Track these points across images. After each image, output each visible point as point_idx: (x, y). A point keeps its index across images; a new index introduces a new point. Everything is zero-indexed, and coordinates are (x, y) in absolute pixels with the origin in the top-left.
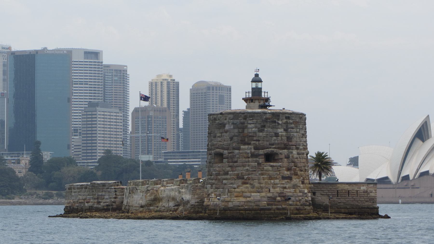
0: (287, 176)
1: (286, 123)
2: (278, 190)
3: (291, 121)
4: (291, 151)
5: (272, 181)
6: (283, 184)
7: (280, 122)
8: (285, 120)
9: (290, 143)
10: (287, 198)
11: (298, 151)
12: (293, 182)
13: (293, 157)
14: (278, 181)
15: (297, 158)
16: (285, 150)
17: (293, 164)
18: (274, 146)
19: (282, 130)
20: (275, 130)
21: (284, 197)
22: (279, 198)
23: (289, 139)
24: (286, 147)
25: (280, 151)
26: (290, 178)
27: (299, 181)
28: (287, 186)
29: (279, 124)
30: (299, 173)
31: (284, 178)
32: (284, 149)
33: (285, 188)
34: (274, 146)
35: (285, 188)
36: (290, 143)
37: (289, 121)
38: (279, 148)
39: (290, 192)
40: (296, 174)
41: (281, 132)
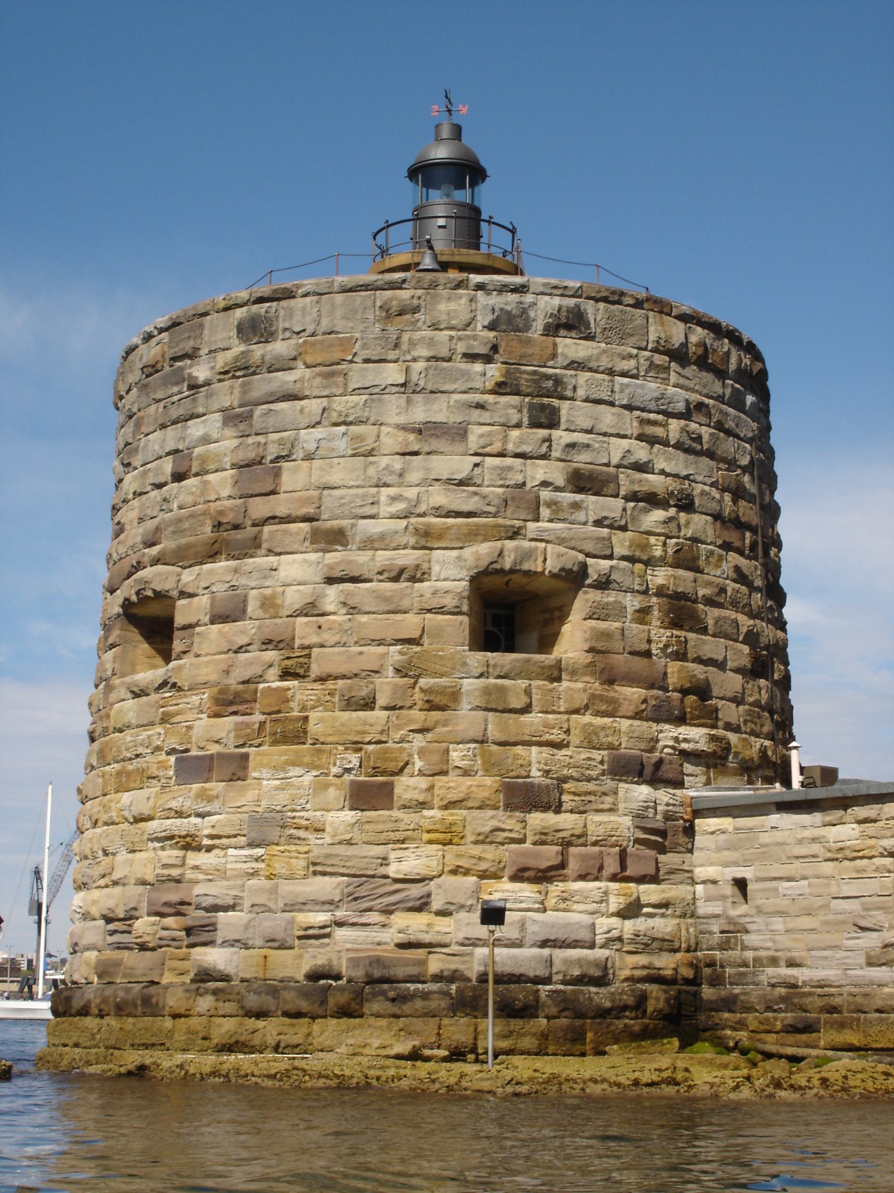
0: (214, 749)
1: (242, 369)
2: (148, 862)
3: (280, 348)
4: (273, 559)
5: (126, 798)
6: (180, 814)
7: (201, 372)
8: (239, 348)
9: (260, 508)
10: (196, 916)
11: (332, 558)
12: (251, 795)
13: (269, 604)
14: (153, 789)
15: (311, 609)
16: (222, 565)
17: (272, 655)
18: (154, 551)
19: (212, 424)
20: (170, 438)
21: (178, 908)
22: (144, 925)
23: (259, 473)
24: (230, 538)
25: (188, 576)
26: (236, 768)
27: (321, 787)
28: (205, 827)
29: (194, 387)
30: (319, 722)
31: (193, 767)
32: (212, 556)
33: (189, 843)
34: (154, 551)
35: (189, 843)
36: (260, 508)
37: (258, 351)
38: (183, 557)
39: (221, 873)
40: (293, 734)
41: (206, 440)
